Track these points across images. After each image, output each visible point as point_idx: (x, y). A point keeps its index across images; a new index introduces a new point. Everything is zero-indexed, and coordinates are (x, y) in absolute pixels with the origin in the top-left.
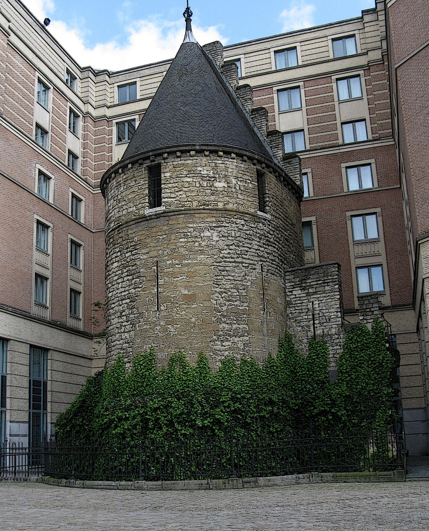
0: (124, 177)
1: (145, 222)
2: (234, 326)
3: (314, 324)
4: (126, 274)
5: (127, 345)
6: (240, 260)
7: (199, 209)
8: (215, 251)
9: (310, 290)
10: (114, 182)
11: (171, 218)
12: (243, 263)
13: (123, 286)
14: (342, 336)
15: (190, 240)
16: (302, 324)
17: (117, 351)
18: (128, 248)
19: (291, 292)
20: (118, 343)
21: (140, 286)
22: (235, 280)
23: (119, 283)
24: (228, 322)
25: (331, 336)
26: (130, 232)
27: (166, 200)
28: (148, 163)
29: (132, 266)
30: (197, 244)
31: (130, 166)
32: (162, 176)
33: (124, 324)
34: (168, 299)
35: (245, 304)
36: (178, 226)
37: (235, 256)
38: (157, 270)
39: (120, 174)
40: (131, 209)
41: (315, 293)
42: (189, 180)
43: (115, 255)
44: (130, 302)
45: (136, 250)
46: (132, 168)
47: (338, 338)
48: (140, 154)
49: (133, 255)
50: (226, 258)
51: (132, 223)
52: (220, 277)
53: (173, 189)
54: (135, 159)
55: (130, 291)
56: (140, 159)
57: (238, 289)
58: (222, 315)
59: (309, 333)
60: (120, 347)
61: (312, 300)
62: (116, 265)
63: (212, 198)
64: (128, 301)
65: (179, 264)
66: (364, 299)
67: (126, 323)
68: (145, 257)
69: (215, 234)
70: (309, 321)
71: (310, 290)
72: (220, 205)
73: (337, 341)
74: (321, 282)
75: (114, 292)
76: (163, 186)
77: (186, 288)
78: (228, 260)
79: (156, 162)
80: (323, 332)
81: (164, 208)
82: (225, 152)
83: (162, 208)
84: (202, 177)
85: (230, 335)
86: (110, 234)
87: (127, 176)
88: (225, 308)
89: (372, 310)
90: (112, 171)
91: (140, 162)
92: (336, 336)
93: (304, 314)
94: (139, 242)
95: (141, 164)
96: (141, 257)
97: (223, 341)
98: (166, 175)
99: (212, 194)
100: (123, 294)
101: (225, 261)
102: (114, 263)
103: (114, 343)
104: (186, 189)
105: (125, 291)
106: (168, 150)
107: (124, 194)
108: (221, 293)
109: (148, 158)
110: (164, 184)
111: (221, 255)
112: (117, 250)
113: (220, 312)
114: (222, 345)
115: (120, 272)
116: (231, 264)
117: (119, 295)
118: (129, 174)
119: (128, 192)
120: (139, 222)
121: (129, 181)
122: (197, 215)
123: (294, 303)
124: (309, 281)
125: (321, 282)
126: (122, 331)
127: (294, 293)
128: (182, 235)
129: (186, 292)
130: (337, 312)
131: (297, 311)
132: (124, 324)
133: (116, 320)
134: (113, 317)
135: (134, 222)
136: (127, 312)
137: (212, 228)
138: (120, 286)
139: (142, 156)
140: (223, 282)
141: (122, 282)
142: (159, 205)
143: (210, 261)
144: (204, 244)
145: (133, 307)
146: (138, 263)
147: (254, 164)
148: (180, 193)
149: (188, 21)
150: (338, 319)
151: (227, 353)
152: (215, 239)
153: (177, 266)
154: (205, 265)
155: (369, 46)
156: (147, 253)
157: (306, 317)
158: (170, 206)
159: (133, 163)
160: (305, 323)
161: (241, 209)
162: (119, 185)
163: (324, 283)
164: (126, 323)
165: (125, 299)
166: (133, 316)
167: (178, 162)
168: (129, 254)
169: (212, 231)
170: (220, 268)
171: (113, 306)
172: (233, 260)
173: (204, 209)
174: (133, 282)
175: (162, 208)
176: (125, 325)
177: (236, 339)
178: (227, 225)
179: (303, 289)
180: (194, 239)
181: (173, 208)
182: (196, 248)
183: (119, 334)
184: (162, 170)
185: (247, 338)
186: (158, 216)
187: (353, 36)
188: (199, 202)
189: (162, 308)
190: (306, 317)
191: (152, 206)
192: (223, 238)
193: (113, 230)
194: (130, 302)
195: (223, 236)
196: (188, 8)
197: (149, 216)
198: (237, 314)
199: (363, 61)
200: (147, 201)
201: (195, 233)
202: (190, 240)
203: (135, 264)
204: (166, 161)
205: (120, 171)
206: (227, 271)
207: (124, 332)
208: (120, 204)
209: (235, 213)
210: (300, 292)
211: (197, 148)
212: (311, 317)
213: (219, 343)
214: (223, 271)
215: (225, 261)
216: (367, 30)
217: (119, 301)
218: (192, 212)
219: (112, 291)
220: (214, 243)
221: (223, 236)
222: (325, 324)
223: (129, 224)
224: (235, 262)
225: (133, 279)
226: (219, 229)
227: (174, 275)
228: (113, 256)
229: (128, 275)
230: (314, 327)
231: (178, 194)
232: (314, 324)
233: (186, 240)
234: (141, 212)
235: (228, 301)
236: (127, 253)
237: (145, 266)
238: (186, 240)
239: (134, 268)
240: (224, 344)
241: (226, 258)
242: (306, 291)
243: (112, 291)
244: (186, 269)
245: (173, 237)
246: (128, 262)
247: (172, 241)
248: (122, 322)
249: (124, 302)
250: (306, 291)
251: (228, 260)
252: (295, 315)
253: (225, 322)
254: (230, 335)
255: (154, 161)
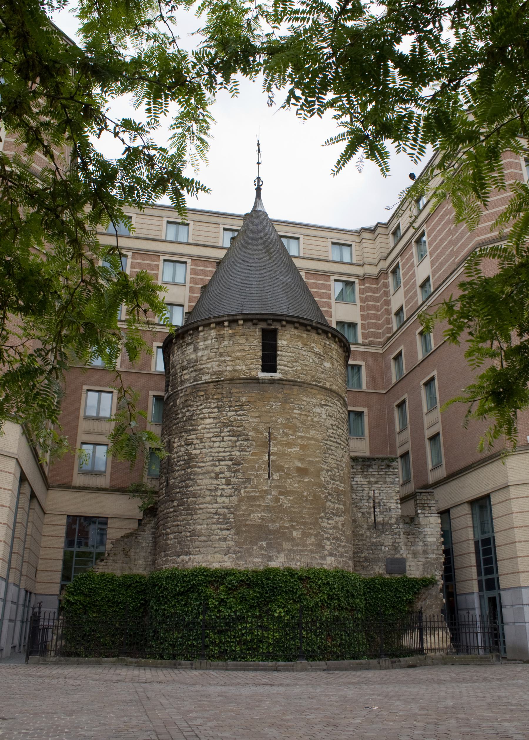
0: (230, 331)
1: (256, 385)
2: (337, 505)
3: (374, 511)
4: (228, 434)
5: (226, 510)
6: (339, 441)
7: (313, 385)
8: (324, 428)
9: (372, 479)
10: (213, 333)
11: (286, 386)
12: (340, 444)
13: (222, 446)
14: (401, 526)
15: (303, 413)
16: (363, 510)
17: (208, 515)
18: (230, 407)
19: (353, 478)
20: (210, 506)
21: (248, 450)
22: (337, 461)
23: (214, 442)
24: (333, 500)
25: (391, 525)
26: (234, 390)
27: (282, 367)
28: (263, 325)
29: (238, 427)
30: (309, 418)
31: (241, 322)
32: (279, 342)
33: (220, 487)
34: (280, 469)
35: (343, 485)
36: (292, 397)
37: (337, 437)
38: (270, 436)
39: (224, 327)
40: (239, 368)
41: (376, 482)
42: (304, 353)
43: (209, 410)
44: (233, 464)
45: (242, 410)
46: (243, 325)
47: (397, 528)
48: (257, 314)
49: (239, 415)
50: (331, 437)
51: (238, 381)
52: (327, 455)
53: (290, 359)
54: (249, 317)
55: (233, 453)
56: (256, 319)
57: (338, 469)
58: (328, 493)
59: (369, 520)
60: (213, 511)
61: (373, 489)
62: (208, 421)
63: (323, 376)
64: (230, 463)
65: (293, 435)
66: (423, 494)
67: (224, 487)
68: (255, 420)
69: (324, 412)
70: (370, 509)
71: (372, 479)
72: (328, 386)
73: (397, 530)
74: (382, 473)
75: (205, 450)
76: (279, 353)
77: (300, 460)
78: (332, 439)
79: (273, 327)
80: (383, 520)
81: (280, 375)
82: (332, 334)
83: (277, 375)
84: (316, 354)
85: (333, 513)
86: (199, 386)
87: (234, 331)
88: (330, 486)
89: (430, 505)
90: (213, 320)
91: (255, 321)
92: (396, 526)
93: (365, 501)
94: (247, 404)
95: (255, 324)
96: (250, 420)
97: (328, 519)
98: (282, 342)
99: (323, 372)
100: (221, 454)
101: (331, 441)
102: (206, 418)
103: (201, 506)
104: (301, 362)
105: (224, 452)
106: (288, 319)
107: (229, 349)
108: (328, 471)
109: (265, 320)
110: (281, 351)
111: (328, 434)
112: (213, 406)
113: (326, 489)
114: (328, 523)
115: (218, 430)
116: (334, 444)
117: (213, 454)
118: (239, 329)
119: (236, 348)
120: (248, 383)
121: (237, 338)
122: (309, 390)
123: (355, 489)
124: (371, 470)
125: (382, 473)
126: (219, 493)
127: (356, 479)
128: (296, 406)
129: (299, 465)
130: (397, 503)
131: (358, 498)
132: (220, 487)
133: (207, 481)
134: (200, 477)
135: (242, 381)
136: (227, 474)
137: (321, 406)
138: (217, 444)
139: (258, 317)
140: (330, 460)
141: (220, 442)
142: (275, 371)
143: (319, 437)
144: (315, 419)
145: (237, 471)
146: (246, 425)
147: (344, 351)
148: (297, 364)
149: (258, 189)
150: (398, 510)
151: (331, 531)
152: (324, 416)
153: (291, 437)
154: (316, 440)
155: (366, 260)
156: (259, 417)
157: (367, 504)
158: (287, 374)
159: (245, 320)
160: (365, 510)
161: (340, 391)
162: (220, 338)
163: (386, 474)
164: (224, 487)
165: (225, 460)
166: (236, 480)
167: (294, 332)
168: (234, 413)
169: (321, 409)
170: (328, 446)
171: (202, 464)
172: (335, 440)
173: (316, 385)
174: (238, 443)
175: (277, 375)
176: (223, 489)
177: (338, 518)
178: (332, 405)
179: (365, 477)
180: (306, 413)
181: (289, 377)
182: (309, 423)
183: (211, 497)
184: (279, 337)
185: (343, 519)
186: (272, 382)
187: (350, 246)
188: (312, 377)
189: (275, 477)
190: (367, 504)
191: (265, 369)
192: (329, 418)
193: (206, 383)
194: (233, 464)
195: (329, 416)
196: (258, 178)
197: (262, 379)
198: (338, 493)
199: (359, 271)
200: (260, 363)
201: (308, 407)
202: (303, 413)
203: (242, 426)
204: (283, 328)
205: (226, 324)
206: (332, 450)
207: (222, 496)
208: (222, 358)
209: (335, 395)
210: (362, 479)
211: (314, 324)
212: (372, 505)
213: (326, 521)
214: (330, 449)
215: (331, 441)
216: (364, 245)
217: (213, 460)
218: (306, 385)
219: (201, 449)
220: (323, 420)
221: (329, 416)
222: (385, 513)
223: (234, 382)
224: (336, 442)
225: (238, 440)
226: (327, 408)
227: (289, 445)
228: (205, 411)
229: (230, 436)
230: (375, 515)
231: (295, 364)
232: (374, 511)
233: (299, 412)
234: (253, 373)
235: (333, 479)
236: (229, 411)
237: (255, 429)
238: (299, 412)
239: (240, 429)
240: (330, 522)
241: (331, 437)
242: (368, 480)
243: (201, 449)
244: (299, 441)
245: (287, 406)
246: (231, 421)
247: (286, 410)
248: (219, 485)
249: (222, 463)
250: (368, 480)
251: (332, 439)
252: (356, 501)
253: (330, 500)
254: (333, 513)
255: (271, 325)
